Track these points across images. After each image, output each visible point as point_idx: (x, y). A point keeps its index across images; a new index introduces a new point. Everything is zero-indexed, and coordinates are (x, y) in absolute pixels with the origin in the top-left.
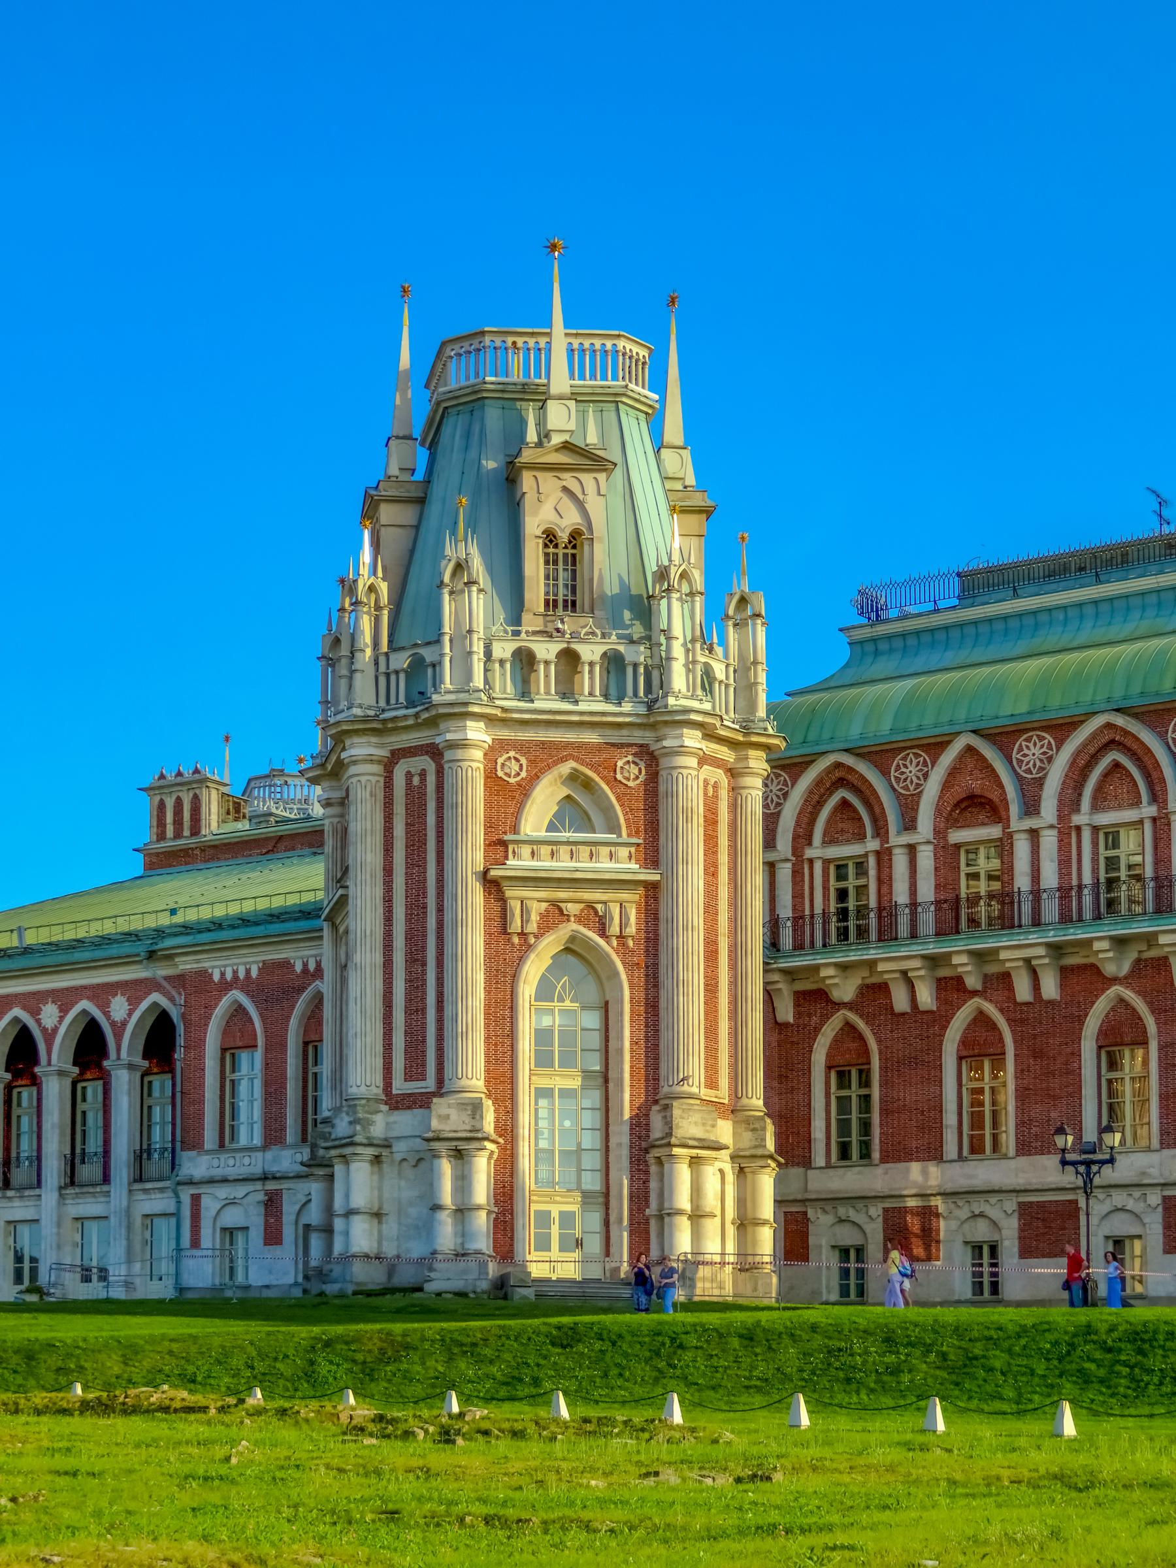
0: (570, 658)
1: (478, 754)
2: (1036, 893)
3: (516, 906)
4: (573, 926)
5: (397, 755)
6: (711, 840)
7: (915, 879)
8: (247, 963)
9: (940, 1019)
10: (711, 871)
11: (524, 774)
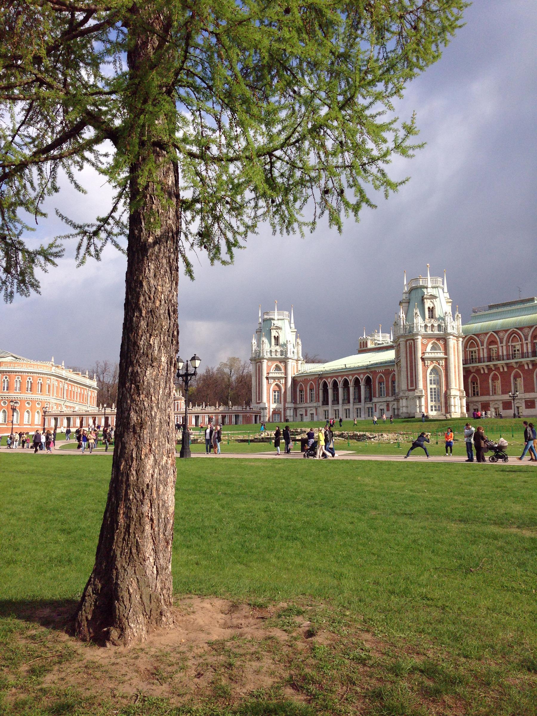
0: (433, 326)
2: (503, 355)
5: (407, 340)
6: (454, 351)
7: (484, 354)
8: (383, 370)
9: (489, 374)
10: (455, 355)
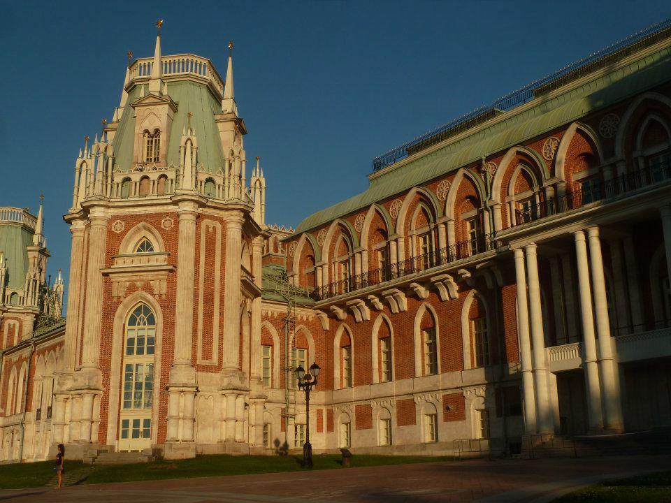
1: (104, 223)
3: (115, 286)
4: (140, 292)
9: (370, 324)
11: (123, 229)
